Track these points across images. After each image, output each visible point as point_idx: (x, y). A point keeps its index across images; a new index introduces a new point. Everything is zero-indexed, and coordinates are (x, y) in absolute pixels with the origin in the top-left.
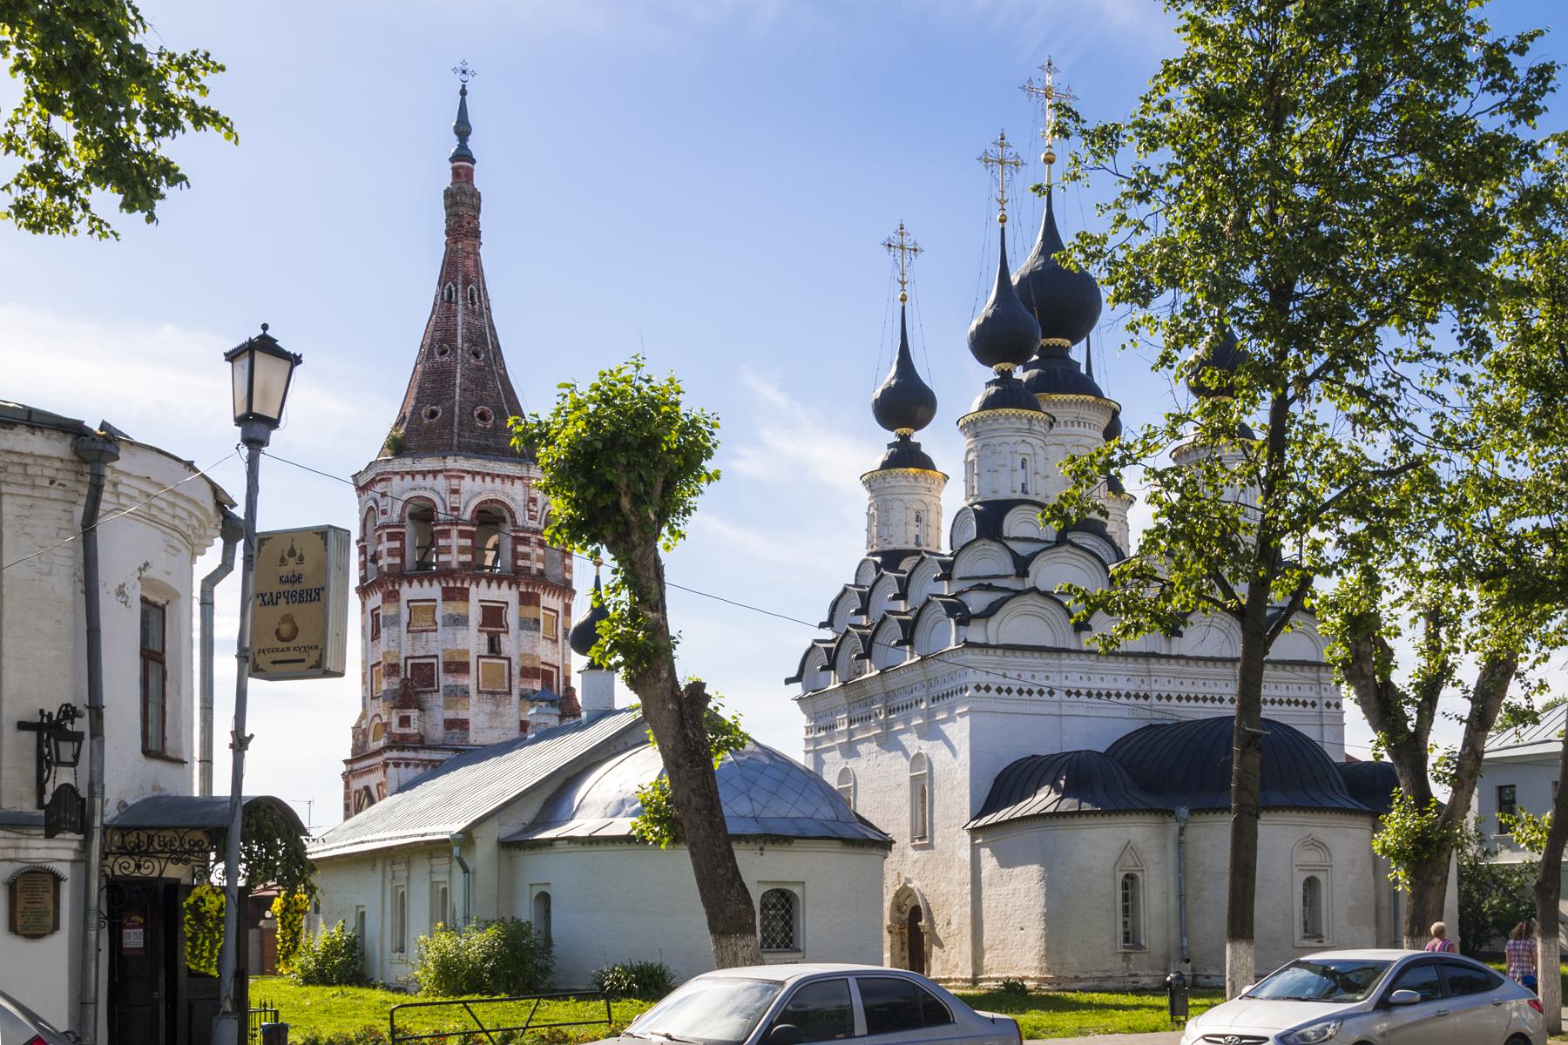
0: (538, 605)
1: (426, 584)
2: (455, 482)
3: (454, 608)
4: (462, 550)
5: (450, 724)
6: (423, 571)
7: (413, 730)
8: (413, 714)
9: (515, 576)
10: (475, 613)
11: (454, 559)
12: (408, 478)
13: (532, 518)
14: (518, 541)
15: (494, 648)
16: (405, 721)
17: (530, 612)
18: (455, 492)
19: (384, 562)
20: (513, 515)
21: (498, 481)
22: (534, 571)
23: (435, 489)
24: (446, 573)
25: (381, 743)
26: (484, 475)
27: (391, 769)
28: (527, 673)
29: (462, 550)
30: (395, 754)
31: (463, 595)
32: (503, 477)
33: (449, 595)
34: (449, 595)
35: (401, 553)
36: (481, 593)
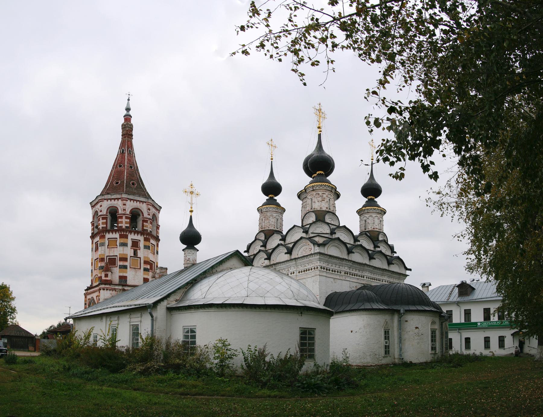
0: (150, 242)
1: (114, 233)
3: (123, 240)
4: (126, 223)
5: (121, 278)
6: (112, 230)
7: (109, 278)
8: (109, 273)
9: (143, 232)
10: (130, 243)
11: (124, 225)
12: (109, 201)
13: (149, 215)
14: (144, 221)
15: (135, 253)
16: (106, 276)
17: (147, 244)
18: (125, 205)
19: (100, 227)
20: (142, 213)
21: (138, 202)
22: (149, 231)
23: (119, 204)
24: (120, 229)
25: (98, 283)
26: (134, 200)
27: (102, 291)
28: (146, 262)
29: (126, 223)
30: (103, 286)
31: (127, 237)
32: (140, 201)
33: (121, 236)
35: (106, 223)
36: (132, 237)
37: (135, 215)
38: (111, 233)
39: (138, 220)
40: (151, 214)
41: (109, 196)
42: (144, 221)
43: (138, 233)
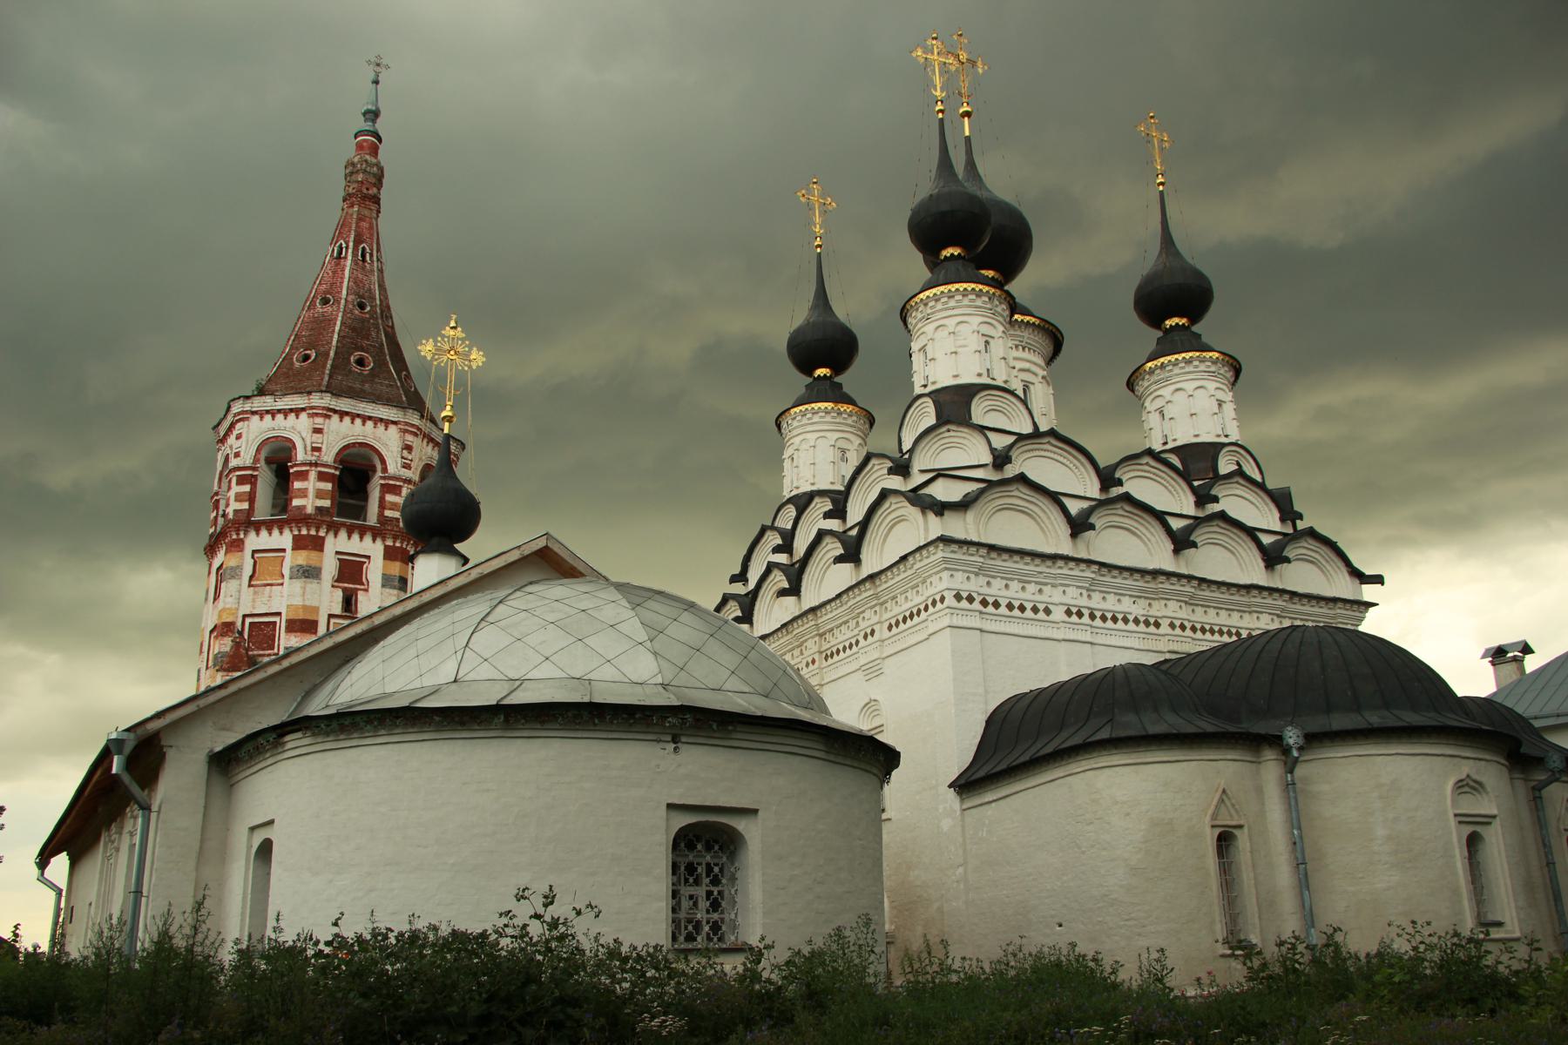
1: (276, 532)
2: (319, 420)
3: (302, 558)
10: (330, 567)
13: (407, 466)
14: (387, 489)
18: (318, 431)
23: (298, 430)
24: (301, 519)
29: (320, 494)
31: (317, 544)
33: (299, 543)
34: (299, 543)
35: (251, 497)
36: (339, 544)
38: (264, 533)
41: (267, 402)
43: (363, 531)
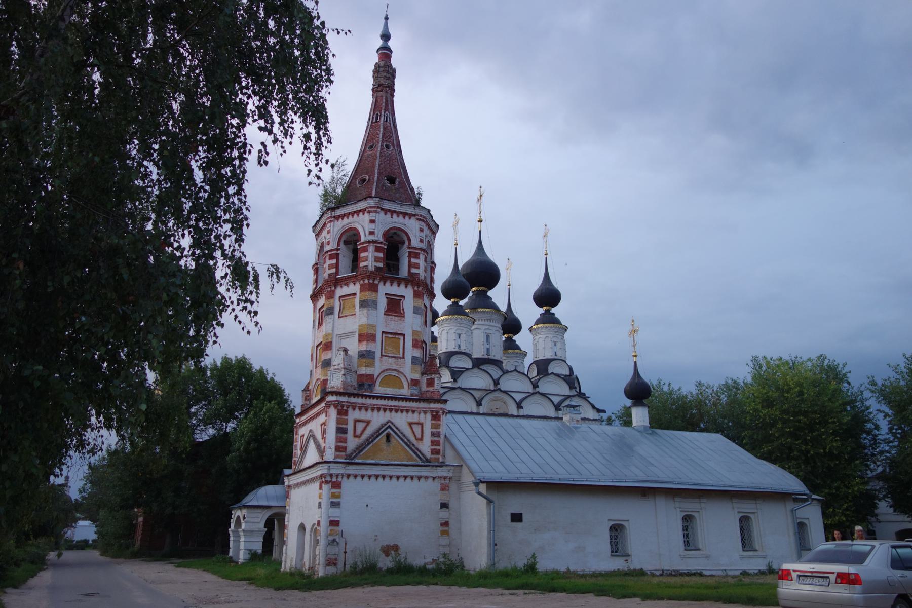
9: (412, 280)
17: (420, 303)
35: (337, 266)
37: (393, 244)
39: (399, 254)
40: (425, 241)
42: (411, 255)
43: (400, 281)
